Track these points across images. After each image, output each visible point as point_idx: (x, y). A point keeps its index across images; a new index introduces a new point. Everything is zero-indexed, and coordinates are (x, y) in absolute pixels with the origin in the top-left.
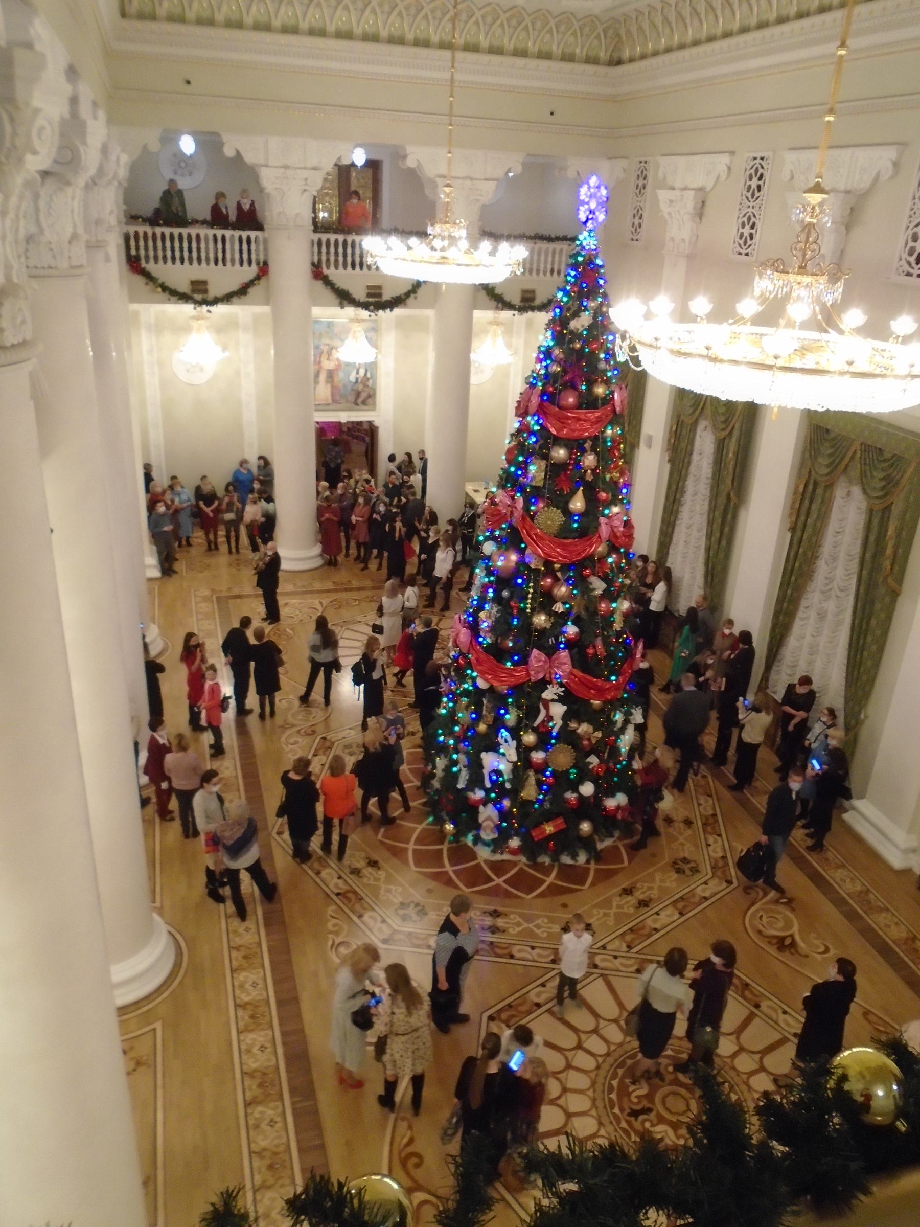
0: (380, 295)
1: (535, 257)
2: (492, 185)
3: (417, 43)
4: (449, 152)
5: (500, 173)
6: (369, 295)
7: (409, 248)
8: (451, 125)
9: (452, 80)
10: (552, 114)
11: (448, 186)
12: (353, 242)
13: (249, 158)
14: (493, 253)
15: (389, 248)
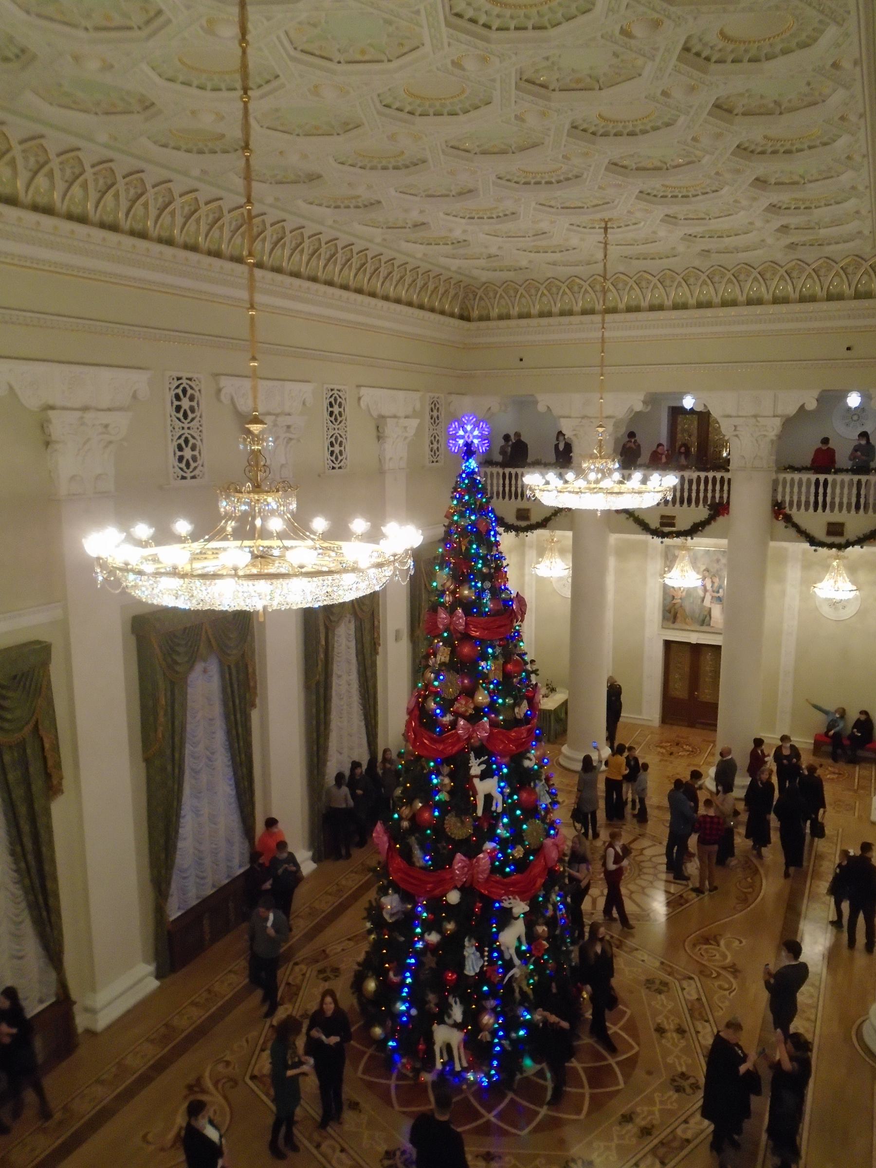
0: (673, 525)
1: (686, 486)
2: (778, 422)
3: (700, 305)
4: (601, 398)
5: (792, 410)
6: (663, 524)
7: (566, 482)
8: (602, 375)
9: (603, 338)
10: (848, 349)
11: (601, 426)
12: (517, 474)
13: (556, 411)
14: (644, 481)
15: (547, 483)
